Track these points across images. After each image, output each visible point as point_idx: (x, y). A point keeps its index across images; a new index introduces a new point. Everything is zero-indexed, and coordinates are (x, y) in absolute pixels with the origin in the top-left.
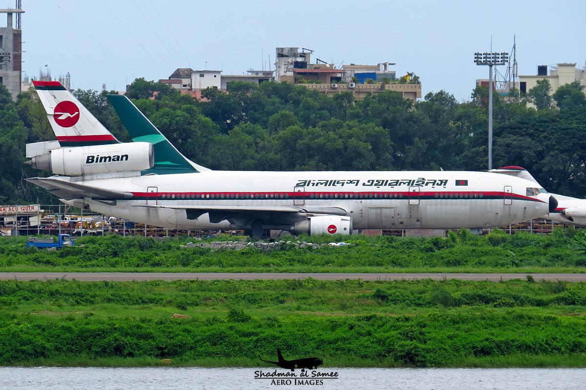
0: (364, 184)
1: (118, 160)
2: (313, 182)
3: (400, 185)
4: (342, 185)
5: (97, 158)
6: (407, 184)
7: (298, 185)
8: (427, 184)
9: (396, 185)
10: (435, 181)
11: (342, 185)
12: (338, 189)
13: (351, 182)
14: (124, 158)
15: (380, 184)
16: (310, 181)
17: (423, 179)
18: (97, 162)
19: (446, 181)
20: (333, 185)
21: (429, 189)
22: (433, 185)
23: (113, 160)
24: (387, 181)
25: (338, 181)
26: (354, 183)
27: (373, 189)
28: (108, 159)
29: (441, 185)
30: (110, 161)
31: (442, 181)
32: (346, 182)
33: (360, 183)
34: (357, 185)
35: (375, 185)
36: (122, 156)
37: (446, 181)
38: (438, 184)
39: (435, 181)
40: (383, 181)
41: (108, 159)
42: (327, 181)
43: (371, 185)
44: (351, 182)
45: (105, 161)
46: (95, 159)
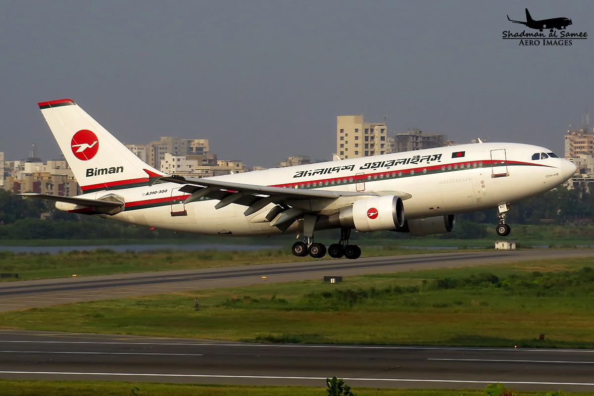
0: (361, 168)
1: (114, 172)
2: (310, 172)
3: (396, 164)
7: (295, 177)
8: (421, 161)
10: (430, 156)
12: (334, 175)
13: (346, 168)
14: (120, 169)
20: (329, 172)
21: (424, 164)
23: (110, 172)
25: (334, 168)
26: (349, 168)
27: (370, 171)
29: (435, 159)
31: (436, 156)
32: (341, 168)
34: (352, 170)
35: (372, 167)
36: (118, 168)
37: (441, 155)
38: (432, 160)
39: (430, 156)
40: (380, 163)
44: (346, 168)
45: (102, 174)
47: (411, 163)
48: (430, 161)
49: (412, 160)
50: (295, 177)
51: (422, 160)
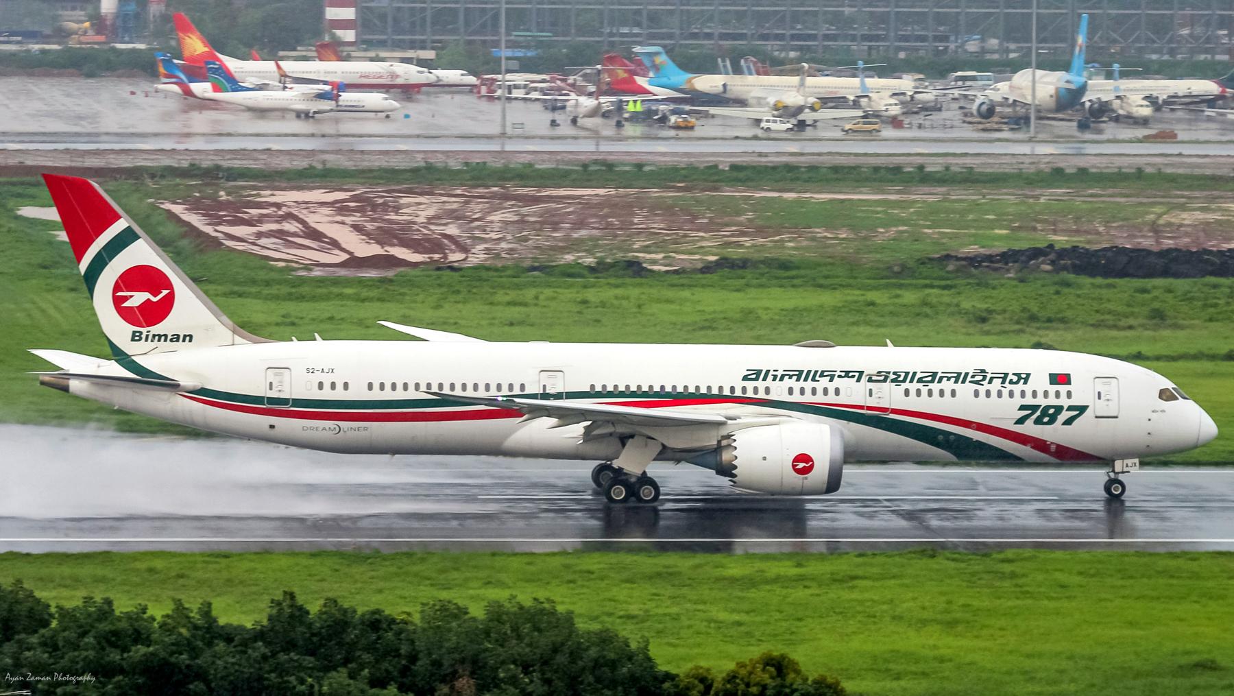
2: (775, 373)
4: (831, 380)
5: (147, 336)
6: (954, 379)
7: (745, 378)
8: (990, 382)
9: (932, 381)
10: (1006, 375)
11: (831, 380)
13: (847, 374)
15: (901, 379)
16: (768, 371)
17: (983, 371)
18: (146, 340)
19: (1028, 375)
20: (813, 380)
22: (1003, 382)
24: (915, 373)
25: (823, 372)
26: (853, 376)
28: (163, 338)
29: (1017, 382)
30: (165, 340)
31: (1018, 375)
33: (864, 379)
37: (1028, 375)
38: (1011, 382)
39: (1006, 375)
40: (907, 374)
41: (163, 338)
42: (801, 372)
43: (885, 381)
44: (847, 374)
45: (159, 340)
46: (144, 336)
47: (970, 382)
48: (1007, 384)
49: (973, 377)
50: (745, 378)
51: (992, 379)
